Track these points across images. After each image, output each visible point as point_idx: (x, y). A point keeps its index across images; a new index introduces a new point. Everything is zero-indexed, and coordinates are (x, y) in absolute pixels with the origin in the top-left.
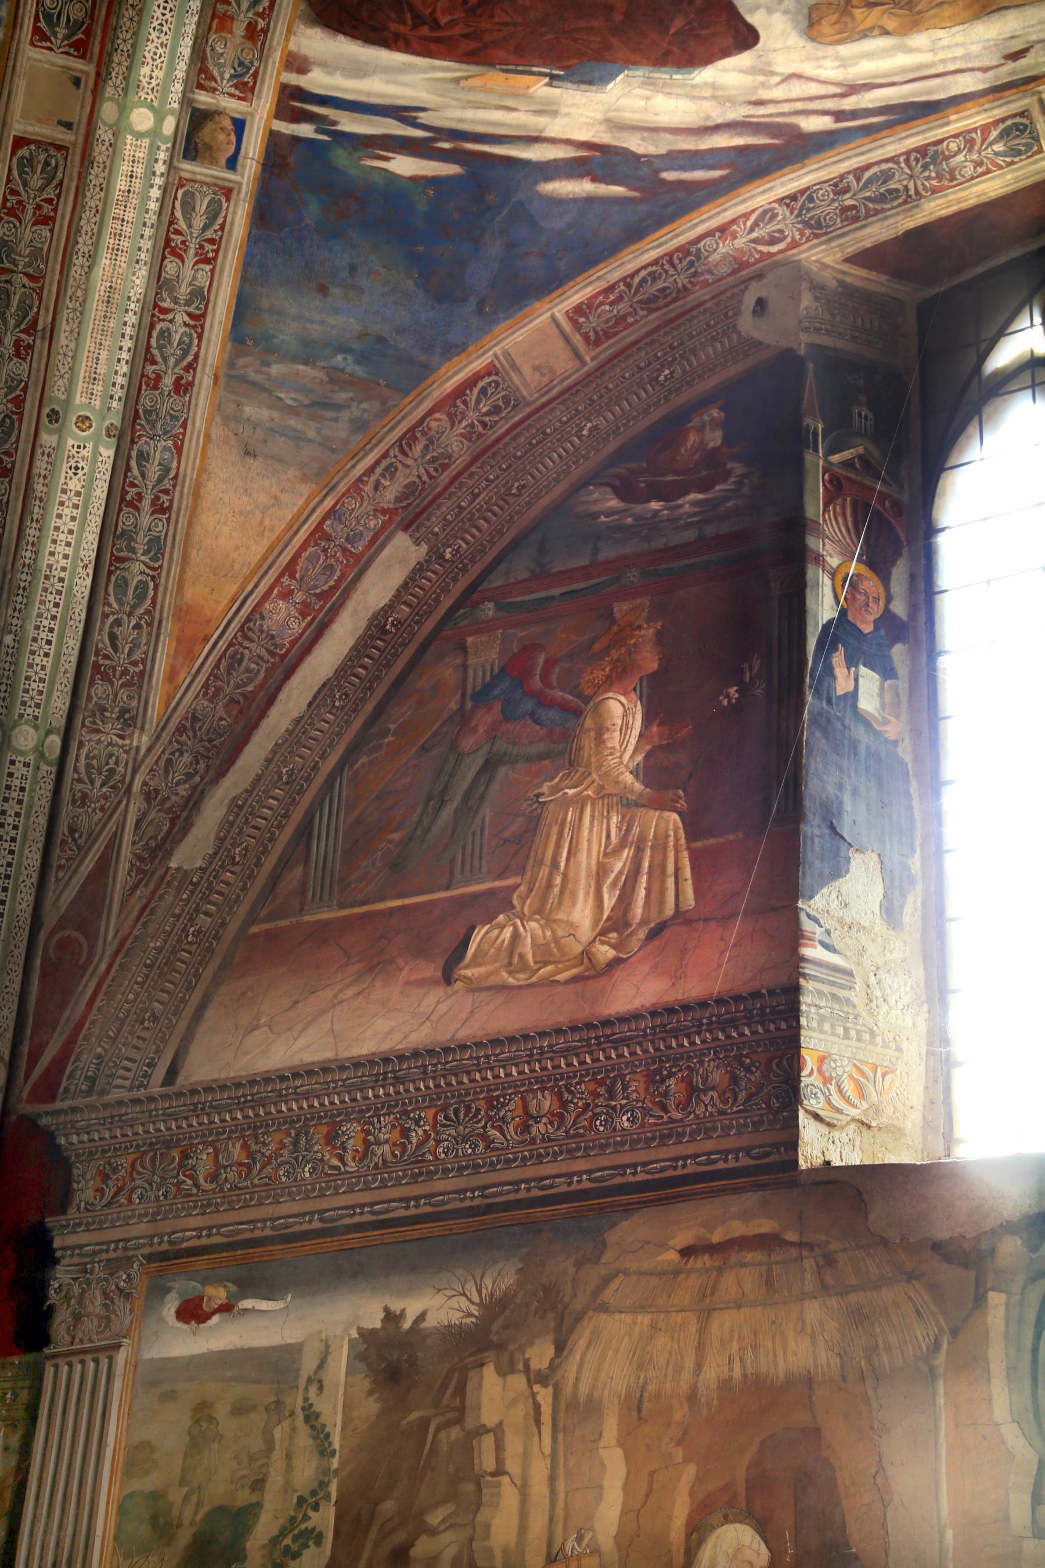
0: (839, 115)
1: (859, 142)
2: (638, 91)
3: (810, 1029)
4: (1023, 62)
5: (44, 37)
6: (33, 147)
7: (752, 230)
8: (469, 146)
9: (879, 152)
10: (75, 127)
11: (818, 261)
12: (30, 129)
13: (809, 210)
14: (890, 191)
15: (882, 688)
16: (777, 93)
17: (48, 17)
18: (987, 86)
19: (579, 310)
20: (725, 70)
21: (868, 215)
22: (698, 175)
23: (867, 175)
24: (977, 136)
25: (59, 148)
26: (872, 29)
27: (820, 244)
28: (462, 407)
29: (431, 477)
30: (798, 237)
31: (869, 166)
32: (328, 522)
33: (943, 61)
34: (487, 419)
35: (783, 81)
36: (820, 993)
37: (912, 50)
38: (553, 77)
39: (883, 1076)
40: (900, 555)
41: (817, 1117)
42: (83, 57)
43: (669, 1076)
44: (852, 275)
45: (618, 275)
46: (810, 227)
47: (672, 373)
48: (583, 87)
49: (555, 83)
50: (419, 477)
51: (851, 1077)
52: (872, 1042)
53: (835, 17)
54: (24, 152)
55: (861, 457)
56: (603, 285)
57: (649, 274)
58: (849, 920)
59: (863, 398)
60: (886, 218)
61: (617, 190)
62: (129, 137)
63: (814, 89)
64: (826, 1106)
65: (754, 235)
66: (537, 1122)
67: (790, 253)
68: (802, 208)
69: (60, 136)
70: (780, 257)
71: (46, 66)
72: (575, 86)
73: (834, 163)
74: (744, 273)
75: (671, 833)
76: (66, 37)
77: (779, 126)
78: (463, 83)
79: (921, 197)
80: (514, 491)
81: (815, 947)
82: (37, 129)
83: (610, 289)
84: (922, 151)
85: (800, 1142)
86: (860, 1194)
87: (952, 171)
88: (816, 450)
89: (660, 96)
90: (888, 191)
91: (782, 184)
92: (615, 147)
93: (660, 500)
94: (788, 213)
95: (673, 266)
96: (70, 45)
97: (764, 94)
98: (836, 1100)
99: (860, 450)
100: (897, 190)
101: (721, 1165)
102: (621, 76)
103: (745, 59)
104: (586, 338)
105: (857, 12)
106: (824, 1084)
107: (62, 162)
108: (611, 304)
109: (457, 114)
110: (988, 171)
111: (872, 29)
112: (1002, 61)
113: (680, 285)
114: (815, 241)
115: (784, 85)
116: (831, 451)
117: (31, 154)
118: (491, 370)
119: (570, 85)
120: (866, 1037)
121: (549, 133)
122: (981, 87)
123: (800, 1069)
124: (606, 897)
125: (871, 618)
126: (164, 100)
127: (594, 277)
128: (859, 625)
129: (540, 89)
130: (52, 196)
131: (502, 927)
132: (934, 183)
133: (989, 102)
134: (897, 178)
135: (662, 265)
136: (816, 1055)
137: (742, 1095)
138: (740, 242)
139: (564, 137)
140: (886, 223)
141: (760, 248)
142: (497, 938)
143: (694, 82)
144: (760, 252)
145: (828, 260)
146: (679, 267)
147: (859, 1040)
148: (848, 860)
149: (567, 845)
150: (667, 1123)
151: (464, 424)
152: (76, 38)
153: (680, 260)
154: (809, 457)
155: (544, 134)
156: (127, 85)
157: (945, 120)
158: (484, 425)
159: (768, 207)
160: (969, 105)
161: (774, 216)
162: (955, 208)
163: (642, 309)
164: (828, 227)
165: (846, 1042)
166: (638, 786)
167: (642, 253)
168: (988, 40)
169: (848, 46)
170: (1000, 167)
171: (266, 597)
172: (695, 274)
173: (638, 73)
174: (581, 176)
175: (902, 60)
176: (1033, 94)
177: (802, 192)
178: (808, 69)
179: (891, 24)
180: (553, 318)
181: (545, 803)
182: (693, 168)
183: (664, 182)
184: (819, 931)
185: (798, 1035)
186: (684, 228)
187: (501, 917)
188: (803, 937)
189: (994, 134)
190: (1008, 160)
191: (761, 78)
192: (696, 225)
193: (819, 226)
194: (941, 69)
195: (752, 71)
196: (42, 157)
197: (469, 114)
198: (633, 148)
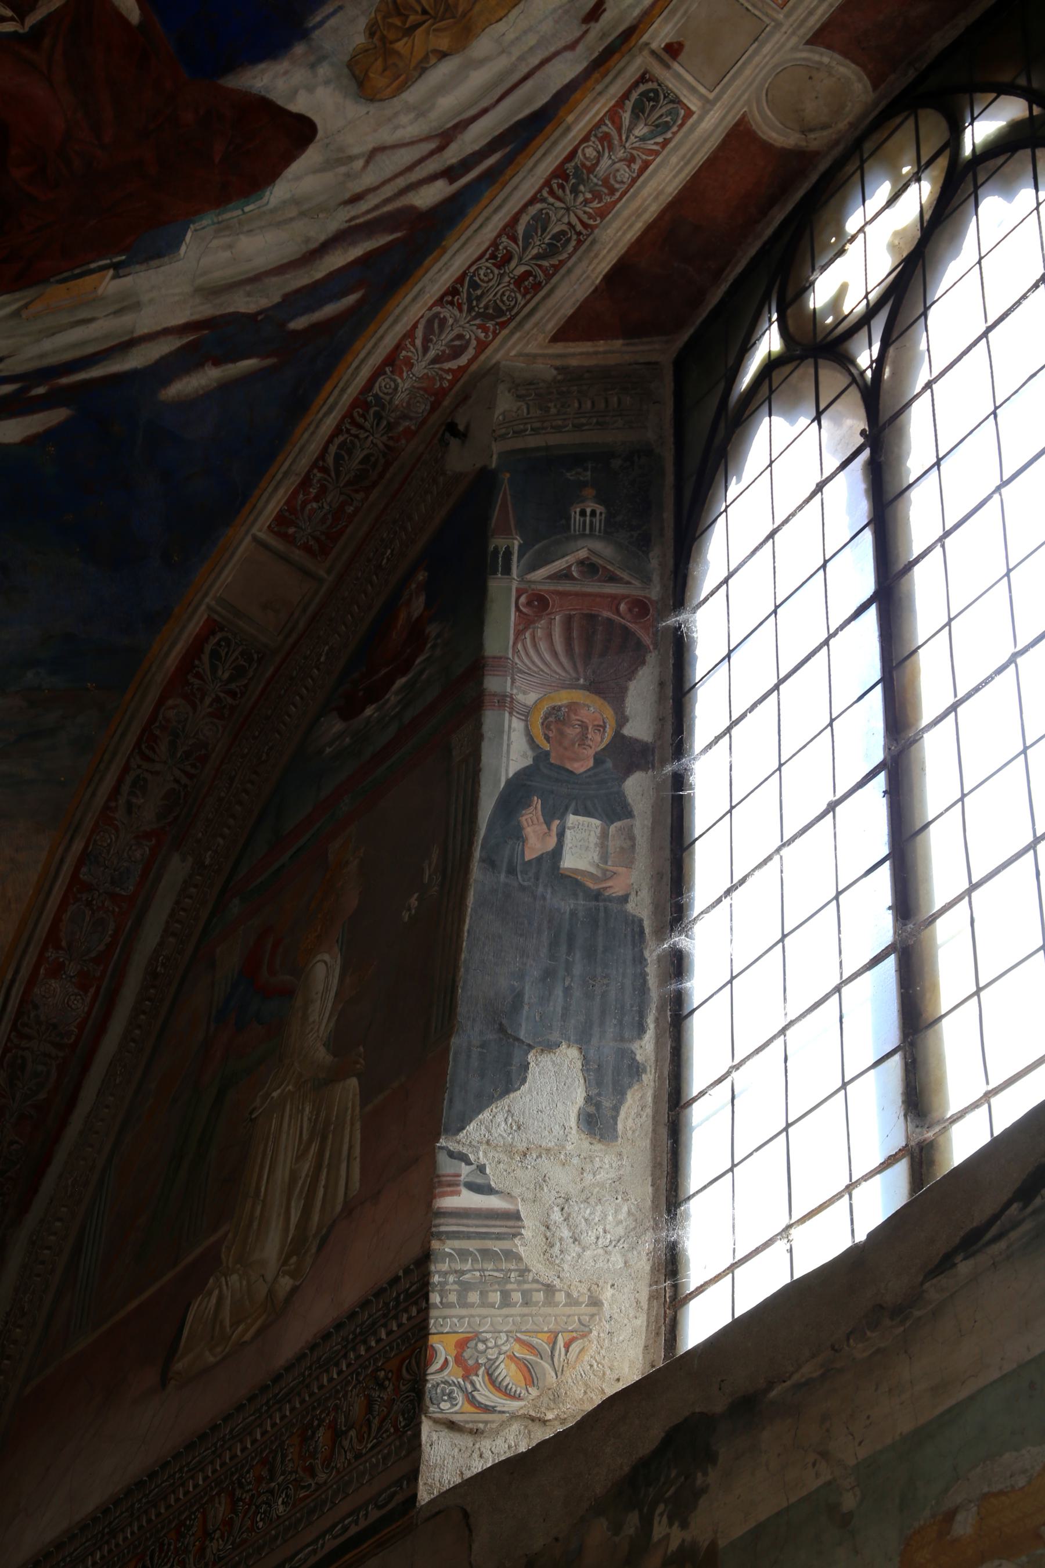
0: (450, 174)
1: (487, 194)
2: (215, 243)
3: (451, 1305)
4: (606, 17)
7: (426, 349)
8: (65, 381)
9: (518, 195)
11: (520, 354)
13: (479, 298)
14: (557, 237)
15: (604, 835)
16: (369, 179)
18: (585, 64)
19: (282, 520)
20: (298, 178)
21: (549, 277)
22: (330, 310)
23: (521, 229)
24: (609, 128)
26: (426, 58)
27: (512, 333)
28: (196, 682)
29: (190, 776)
30: (482, 335)
31: (515, 219)
32: (84, 870)
33: (521, 58)
34: (233, 686)
35: (367, 162)
36: (463, 1254)
37: (481, 63)
38: (116, 266)
39: (567, 1346)
40: (643, 663)
41: (452, 1426)
43: (319, 1426)
44: (573, 355)
45: (304, 464)
46: (491, 318)
47: (392, 551)
48: (154, 263)
49: (121, 272)
50: (177, 781)
51: (513, 1358)
52: (550, 1301)
53: (379, 62)
55: (581, 563)
56: (293, 482)
57: (341, 446)
58: (522, 1147)
59: (589, 492)
60: (569, 271)
61: (249, 364)
63: (406, 157)
64: (468, 1408)
65: (432, 354)
66: (212, 1540)
67: (482, 357)
68: (469, 300)
70: (474, 367)
72: (144, 267)
73: (476, 231)
74: (446, 403)
75: (350, 1105)
77: (390, 215)
78: (25, 314)
79: (592, 228)
80: (264, 757)
81: (458, 1193)
83: (306, 482)
84: (560, 173)
85: (423, 1468)
86: (466, 1515)
87: (606, 182)
88: (507, 571)
89: (242, 237)
90: (553, 238)
91: (433, 281)
92: (222, 316)
93: (372, 703)
94: (457, 313)
95: (360, 427)
97: (356, 187)
98: (486, 1395)
99: (583, 554)
100: (563, 233)
101: (353, 1530)
102: (189, 234)
103: (312, 156)
104: (307, 549)
105: (399, 46)
106: (465, 1378)
108: (316, 499)
109: (33, 351)
110: (646, 165)
111: (426, 58)
112: (584, 27)
113: (381, 445)
114: (505, 332)
115: (371, 166)
116: (533, 567)
118: (212, 627)
119: (138, 267)
120: (540, 1296)
121: (142, 330)
122: (579, 68)
123: (427, 1364)
124: (293, 1211)
125: (591, 752)
127: (279, 476)
128: (568, 766)
129: (109, 285)
131: (210, 1293)
132: (595, 204)
133: (598, 82)
134: (554, 218)
135: (348, 431)
136: (453, 1339)
137: (376, 1422)
138: (420, 368)
139: (159, 328)
140: (573, 277)
141: (447, 366)
142: (206, 1308)
143: (271, 206)
144: (450, 370)
145: (532, 348)
146: (367, 425)
147: (526, 1303)
148: (526, 1067)
149: (268, 1162)
150: (316, 1490)
151: (208, 701)
153: (363, 416)
154: (495, 584)
155: (135, 335)
157: (564, 126)
158: (233, 694)
159: (429, 314)
160: (577, 95)
161: (443, 322)
162: (639, 226)
163: (357, 491)
164: (510, 310)
165: (505, 1311)
166: (329, 1058)
167: (317, 427)
168: (555, 10)
169: (412, 89)
170: (657, 153)
171: (32, 982)
172: (390, 427)
173: (205, 222)
174: (199, 365)
175: (478, 78)
176: (641, 50)
177: (460, 280)
178: (385, 136)
179: (443, 43)
180: (255, 538)
181: (256, 1118)
182: (320, 305)
183: (295, 333)
184: (465, 1170)
185: (426, 1319)
186: (345, 378)
187: (211, 1281)
188: (441, 1184)
189: (626, 117)
190: (660, 140)
191: (343, 170)
192: (358, 368)
193: (500, 313)
194: (524, 70)
195: (328, 165)
197: (48, 345)
198: (243, 309)
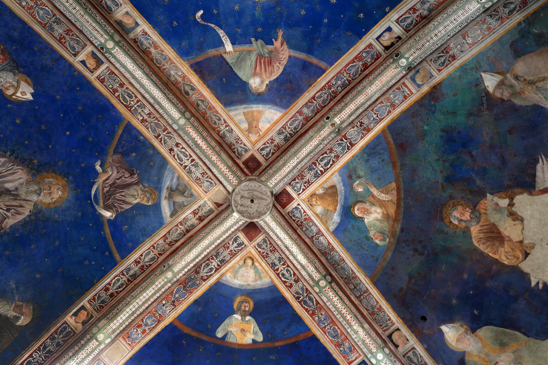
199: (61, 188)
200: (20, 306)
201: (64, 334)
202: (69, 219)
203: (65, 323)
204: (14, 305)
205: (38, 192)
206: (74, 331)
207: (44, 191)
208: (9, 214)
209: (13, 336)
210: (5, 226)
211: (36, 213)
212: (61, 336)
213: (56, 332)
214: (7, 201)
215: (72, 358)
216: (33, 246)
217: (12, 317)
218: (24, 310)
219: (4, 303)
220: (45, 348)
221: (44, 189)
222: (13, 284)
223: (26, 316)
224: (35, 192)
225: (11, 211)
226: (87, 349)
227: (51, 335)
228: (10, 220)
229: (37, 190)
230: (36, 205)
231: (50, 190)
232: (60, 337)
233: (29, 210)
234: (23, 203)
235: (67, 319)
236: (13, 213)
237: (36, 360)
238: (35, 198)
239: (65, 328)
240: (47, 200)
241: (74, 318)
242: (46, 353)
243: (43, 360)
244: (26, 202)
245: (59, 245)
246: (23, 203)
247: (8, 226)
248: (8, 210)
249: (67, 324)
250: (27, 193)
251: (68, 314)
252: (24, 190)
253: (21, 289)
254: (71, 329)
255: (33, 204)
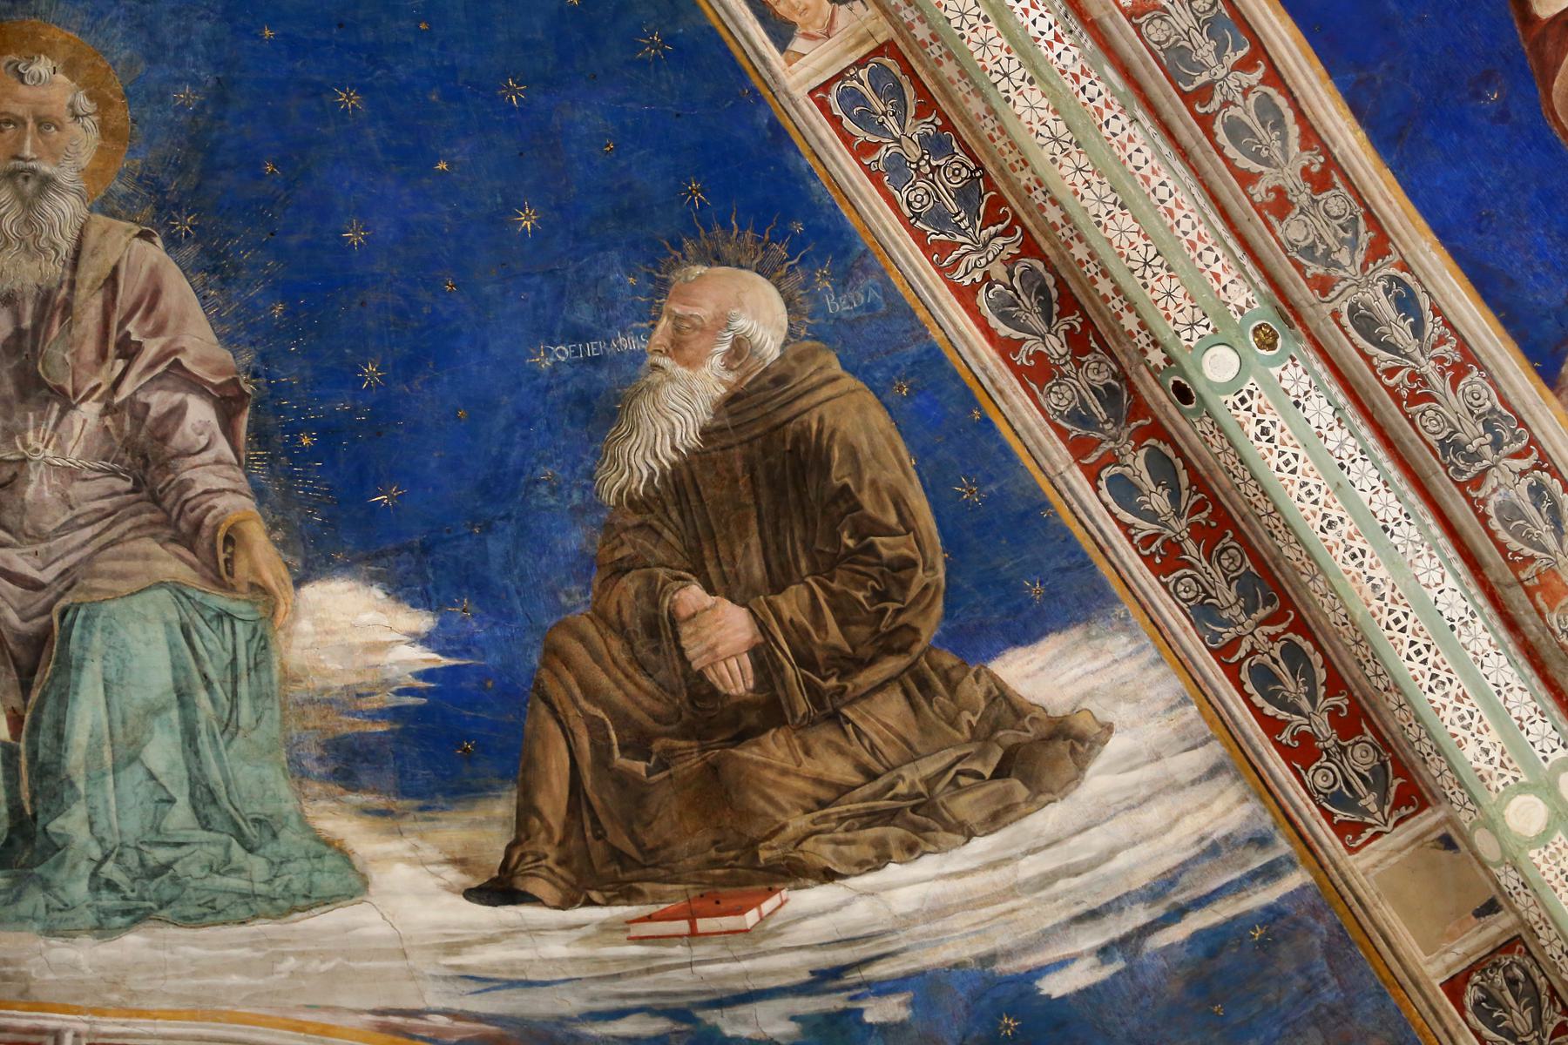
5: (1358, 828)
6: (1476, 978)
10: (1501, 901)
12: (1450, 958)
17: (1337, 799)
25: (1508, 946)
42: (1424, 805)
54: (1471, 995)
62: (1533, 853)
69: (1493, 930)
71: (1394, 860)
76: (1381, 802)
82: (1460, 950)
96: (1396, 806)
107: (1527, 962)
117: (1482, 988)
126: (1530, 764)
130: (1559, 1019)
152: (1393, 790)
156: (1469, 791)
196: (1499, 979)
199: (12, 57)
200: (678, 330)
201: (878, 106)
202: (205, 25)
203: (819, 94)
204: (665, 362)
205: (30, 187)
206: (878, 51)
207: (28, 153)
208: (152, 348)
209: (834, 379)
210: (220, 372)
211: (159, 208)
212: (891, 123)
213: (863, 151)
214: (76, 355)
215: (997, 104)
216: (354, 237)
217: (730, 377)
218: (704, 310)
219: (645, 407)
220: (940, 218)
221: (16, 157)
222: (548, 352)
223: (740, 304)
224: (28, 204)
225: (134, 337)
226: (963, 15)
227: (875, 178)
228: (185, 342)
229: (20, 195)
230: (105, 206)
231: (19, 122)
232: (897, 133)
233: (137, 243)
234: (92, 272)
235: (800, 83)
236: (149, 327)
237: (998, 271)
238: (65, 210)
239: (852, 98)
240: (84, 140)
241: (798, 45)
242: (973, 215)
243: (1008, 232)
244: (85, 254)
245: (362, 90)
246: (91, 275)
247: (224, 355)
248: (129, 351)
249: (825, 86)
250: (33, 250)
251: (774, 76)
252: (16, 265)
253: (583, 314)
254: (861, 63)
255: (100, 220)
